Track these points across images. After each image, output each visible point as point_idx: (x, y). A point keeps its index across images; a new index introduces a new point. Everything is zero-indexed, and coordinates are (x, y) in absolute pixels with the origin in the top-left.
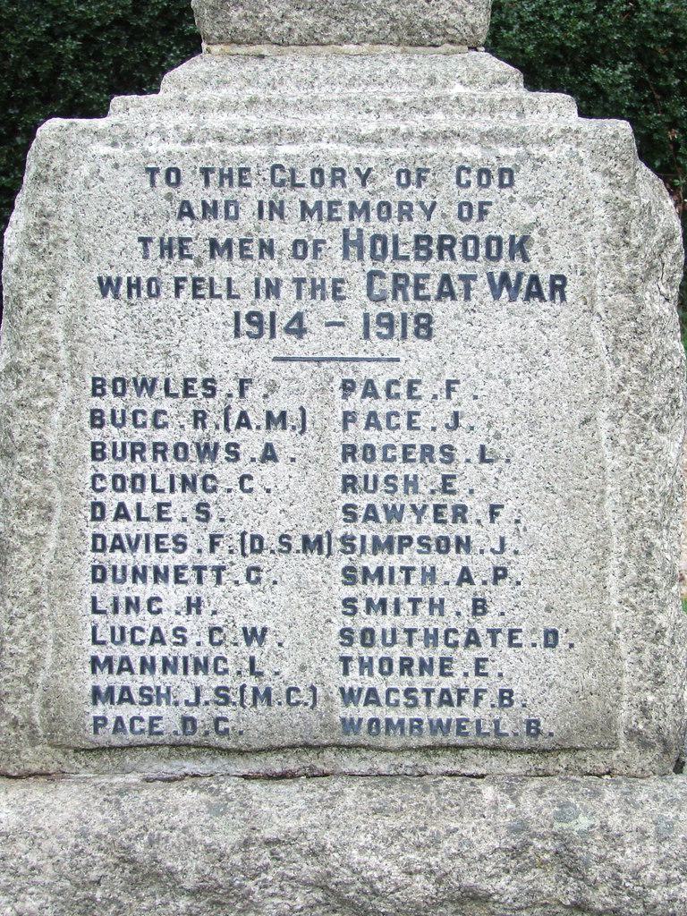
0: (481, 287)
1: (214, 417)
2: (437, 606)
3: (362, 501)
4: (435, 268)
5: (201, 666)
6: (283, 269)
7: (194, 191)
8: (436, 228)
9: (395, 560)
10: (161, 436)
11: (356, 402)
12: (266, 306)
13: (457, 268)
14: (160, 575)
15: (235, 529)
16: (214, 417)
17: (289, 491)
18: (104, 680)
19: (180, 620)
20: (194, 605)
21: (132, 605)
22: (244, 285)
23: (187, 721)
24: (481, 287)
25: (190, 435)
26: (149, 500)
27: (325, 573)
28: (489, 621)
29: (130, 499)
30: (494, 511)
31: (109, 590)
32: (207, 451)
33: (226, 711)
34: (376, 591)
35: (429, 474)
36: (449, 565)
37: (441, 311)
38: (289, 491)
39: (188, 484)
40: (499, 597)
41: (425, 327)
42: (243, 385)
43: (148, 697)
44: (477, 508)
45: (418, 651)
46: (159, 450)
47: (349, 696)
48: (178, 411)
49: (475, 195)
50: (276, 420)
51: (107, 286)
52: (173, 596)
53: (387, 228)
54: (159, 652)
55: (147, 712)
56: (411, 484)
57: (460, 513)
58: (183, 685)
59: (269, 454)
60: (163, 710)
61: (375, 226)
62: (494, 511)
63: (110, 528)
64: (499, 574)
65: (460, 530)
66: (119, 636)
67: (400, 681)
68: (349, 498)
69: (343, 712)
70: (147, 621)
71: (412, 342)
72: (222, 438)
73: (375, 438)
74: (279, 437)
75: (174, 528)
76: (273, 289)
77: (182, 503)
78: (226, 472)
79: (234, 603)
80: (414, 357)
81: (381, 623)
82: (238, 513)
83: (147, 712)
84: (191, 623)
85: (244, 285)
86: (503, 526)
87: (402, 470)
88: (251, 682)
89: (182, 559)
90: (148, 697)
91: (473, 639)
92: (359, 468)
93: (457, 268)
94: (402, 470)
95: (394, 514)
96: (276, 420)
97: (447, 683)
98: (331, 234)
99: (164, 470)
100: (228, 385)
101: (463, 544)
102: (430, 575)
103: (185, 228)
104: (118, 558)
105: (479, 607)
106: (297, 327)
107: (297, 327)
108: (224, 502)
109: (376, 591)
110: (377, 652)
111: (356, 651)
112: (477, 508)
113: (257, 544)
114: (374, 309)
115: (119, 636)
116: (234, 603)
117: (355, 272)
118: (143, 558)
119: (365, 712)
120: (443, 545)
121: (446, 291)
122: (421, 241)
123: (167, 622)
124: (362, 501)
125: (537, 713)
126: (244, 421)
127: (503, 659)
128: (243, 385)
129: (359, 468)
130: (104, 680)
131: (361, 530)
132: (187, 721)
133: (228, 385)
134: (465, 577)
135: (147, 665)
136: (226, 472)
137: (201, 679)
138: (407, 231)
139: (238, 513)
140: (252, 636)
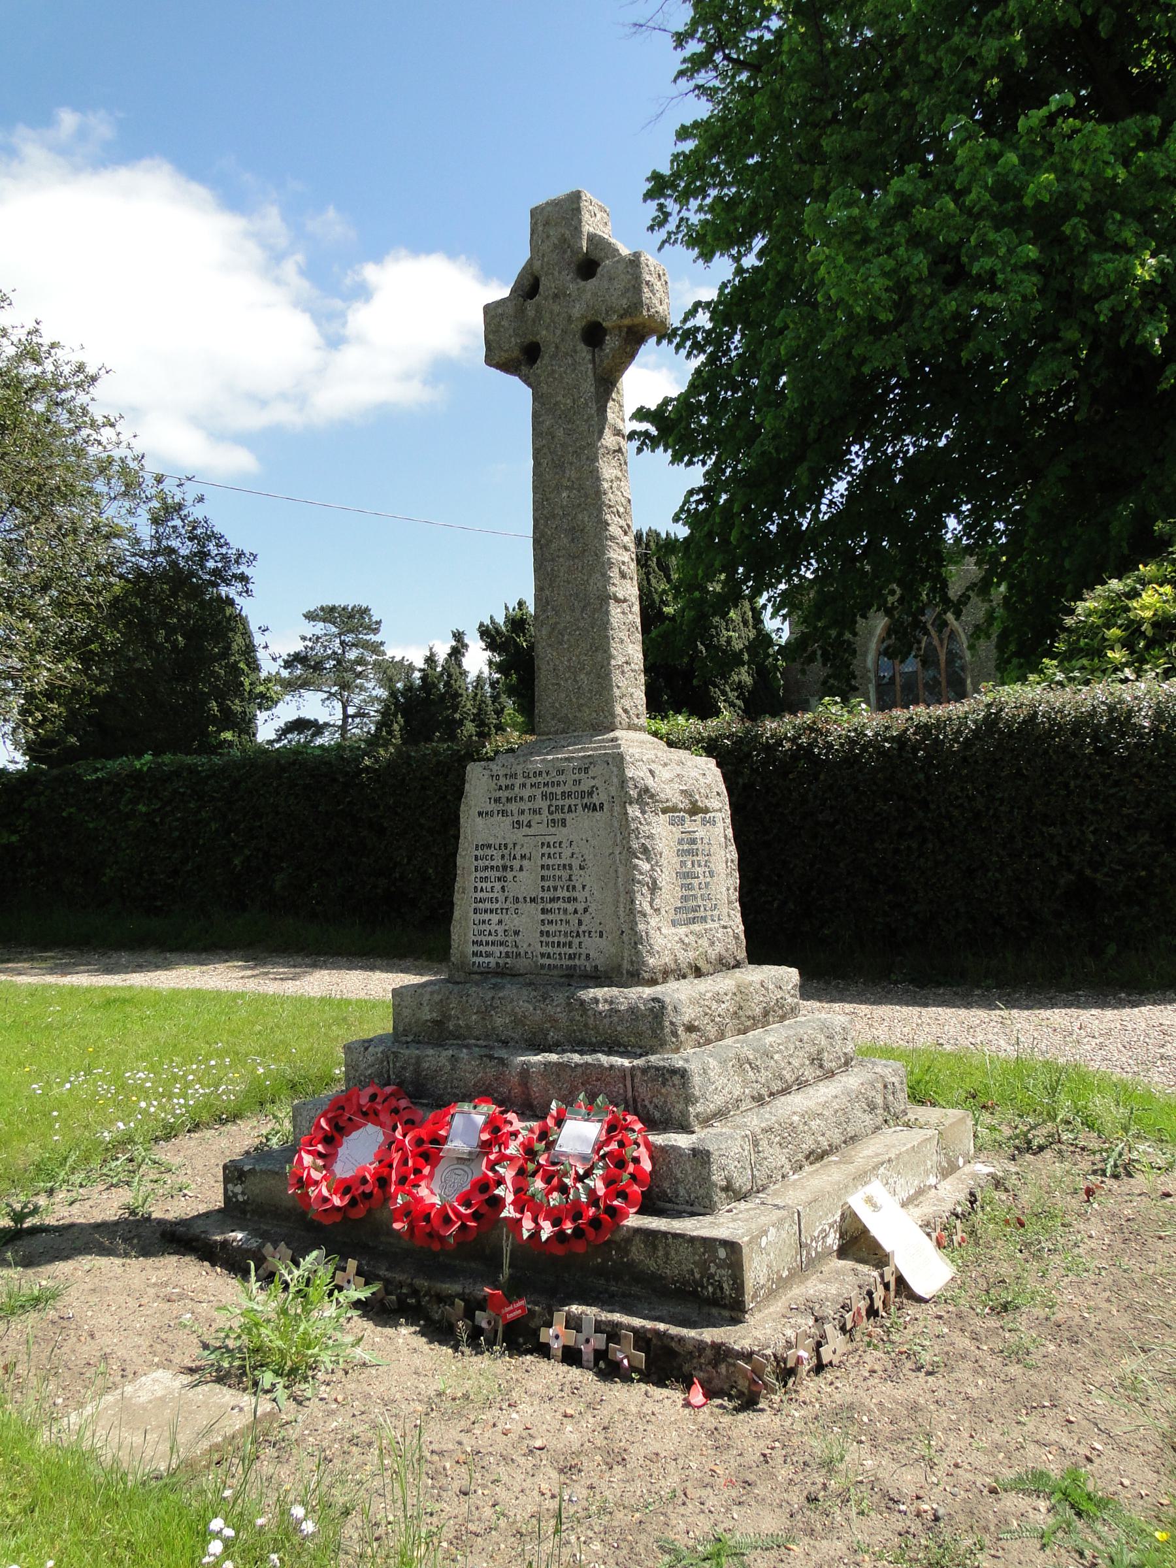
0: (580, 808)
1: (507, 857)
2: (568, 922)
3: (546, 884)
4: (567, 802)
5: (502, 944)
6: (525, 806)
8: (567, 789)
9: (555, 905)
10: (493, 863)
12: (521, 818)
13: (573, 802)
14: (491, 911)
15: (511, 895)
16: (507, 857)
17: (526, 882)
19: (497, 927)
20: (500, 922)
21: (484, 922)
22: (515, 812)
23: (497, 963)
24: (580, 808)
26: (489, 885)
27: (533, 909)
28: (583, 928)
30: (584, 887)
31: (478, 916)
32: (505, 868)
33: (508, 960)
35: (565, 874)
36: (570, 907)
37: (569, 817)
38: (526, 882)
39: (499, 879)
40: (586, 919)
41: (564, 823)
42: (515, 844)
43: (488, 955)
44: (579, 887)
45: (562, 939)
46: (492, 868)
47: (543, 955)
48: (497, 854)
49: (577, 777)
50: (523, 857)
52: (495, 918)
53: (554, 790)
54: (490, 939)
55: (487, 960)
56: (560, 877)
57: (574, 887)
58: (497, 950)
59: (521, 869)
60: (491, 959)
61: (550, 790)
62: (584, 887)
64: (586, 910)
66: (481, 933)
67: (557, 950)
68: (543, 884)
69: (541, 961)
71: (561, 828)
72: (509, 864)
74: (525, 863)
75: (495, 895)
76: (523, 812)
77: (498, 886)
78: (510, 875)
80: (561, 834)
81: (552, 928)
82: (513, 889)
83: (487, 960)
84: (500, 929)
85: (515, 812)
86: (586, 893)
87: (558, 873)
88: (515, 950)
89: (497, 906)
90: (488, 955)
91: (578, 935)
92: (545, 873)
93: (573, 802)
94: (558, 873)
96: (523, 857)
97: (571, 951)
98: (538, 792)
99: (493, 874)
100: (510, 846)
101: (575, 899)
102: (565, 911)
104: (481, 905)
105: (580, 923)
106: (529, 825)
107: (529, 825)
108: (509, 885)
109: (550, 917)
110: (550, 939)
111: (544, 939)
112: (579, 887)
113: (517, 900)
114: (550, 817)
115: (481, 933)
116: (513, 921)
117: (544, 805)
118: (488, 905)
119: (546, 961)
120: (569, 900)
121: (570, 810)
122: (563, 793)
123: (493, 927)
124: (546, 884)
125: (597, 962)
126: (515, 858)
127: (586, 940)
128: (515, 844)
129: (545, 873)
130: (476, 948)
131: (547, 895)
132: (497, 963)
133: (510, 846)
134: (576, 912)
135: (487, 943)
136: (510, 875)
137: (502, 948)
138: (559, 790)
139: (513, 889)
140: (517, 933)
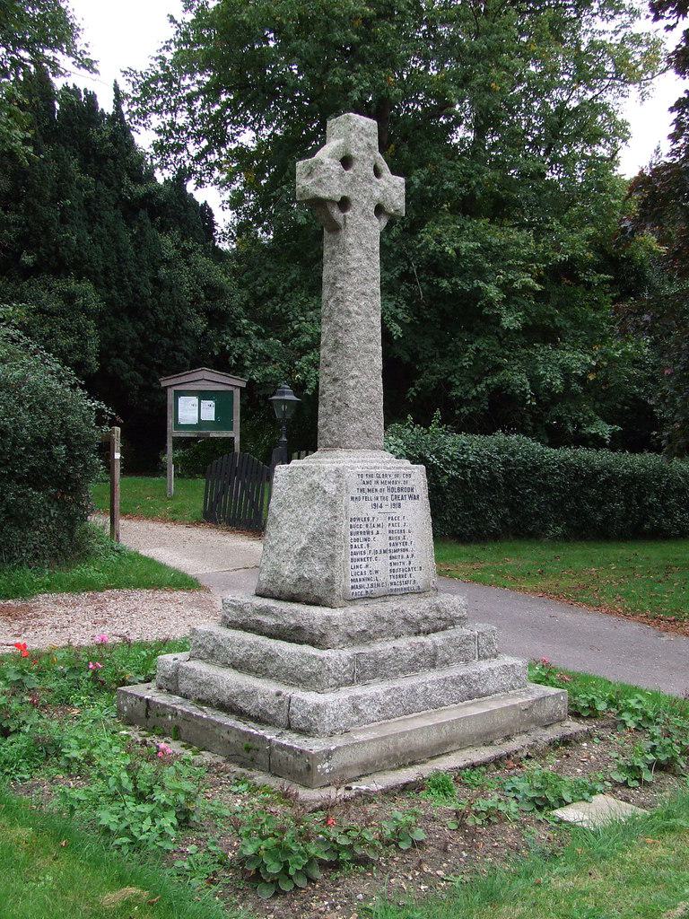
0: (407, 497)
3: (392, 542)
6: (378, 494)
7: (365, 479)
9: (397, 554)
11: (390, 521)
17: (380, 542)
18: (353, 584)
24: (407, 497)
25: (366, 529)
29: (357, 543)
32: (368, 533)
34: (395, 561)
35: (401, 535)
36: (405, 554)
37: (402, 502)
38: (380, 542)
40: (413, 560)
44: (409, 542)
47: (391, 584)
48: (363, 524)
50: (379, 526)
51: (352, 498)
52: (364, 564)
61: (392, 486)
63: (354, 550)
65: (406, 547)
66: (356, 574)
67: (399, 580)
70: (359, 570)
72: (370, 530)
73: (394, 529)
75: (363, 550)
77: (365, 544)
79: (374, 565)
92: (391, 535)
95: (397, 544)
96: (379, 526)
98: (385, 487)
99: (361, 537)
100: (371, 519)
101: (407, 550)
103: (363, 486)
105: (410, 563)
109: (395, 561)
110: (395, 574)
112: (409, 542)
115: (356, 574)
116: (374, 565)
117: (389, 495)
118: (359, 556)
119: (394, 587)
121: (402, 499)
123: (363, 570)
124: (392, 542)
127: (413, 572)
130: (353, 584)
131: (392, 548)
133: (371, 519)
136: (371, 537)
137: (368, 582)
140: (377, 572)
